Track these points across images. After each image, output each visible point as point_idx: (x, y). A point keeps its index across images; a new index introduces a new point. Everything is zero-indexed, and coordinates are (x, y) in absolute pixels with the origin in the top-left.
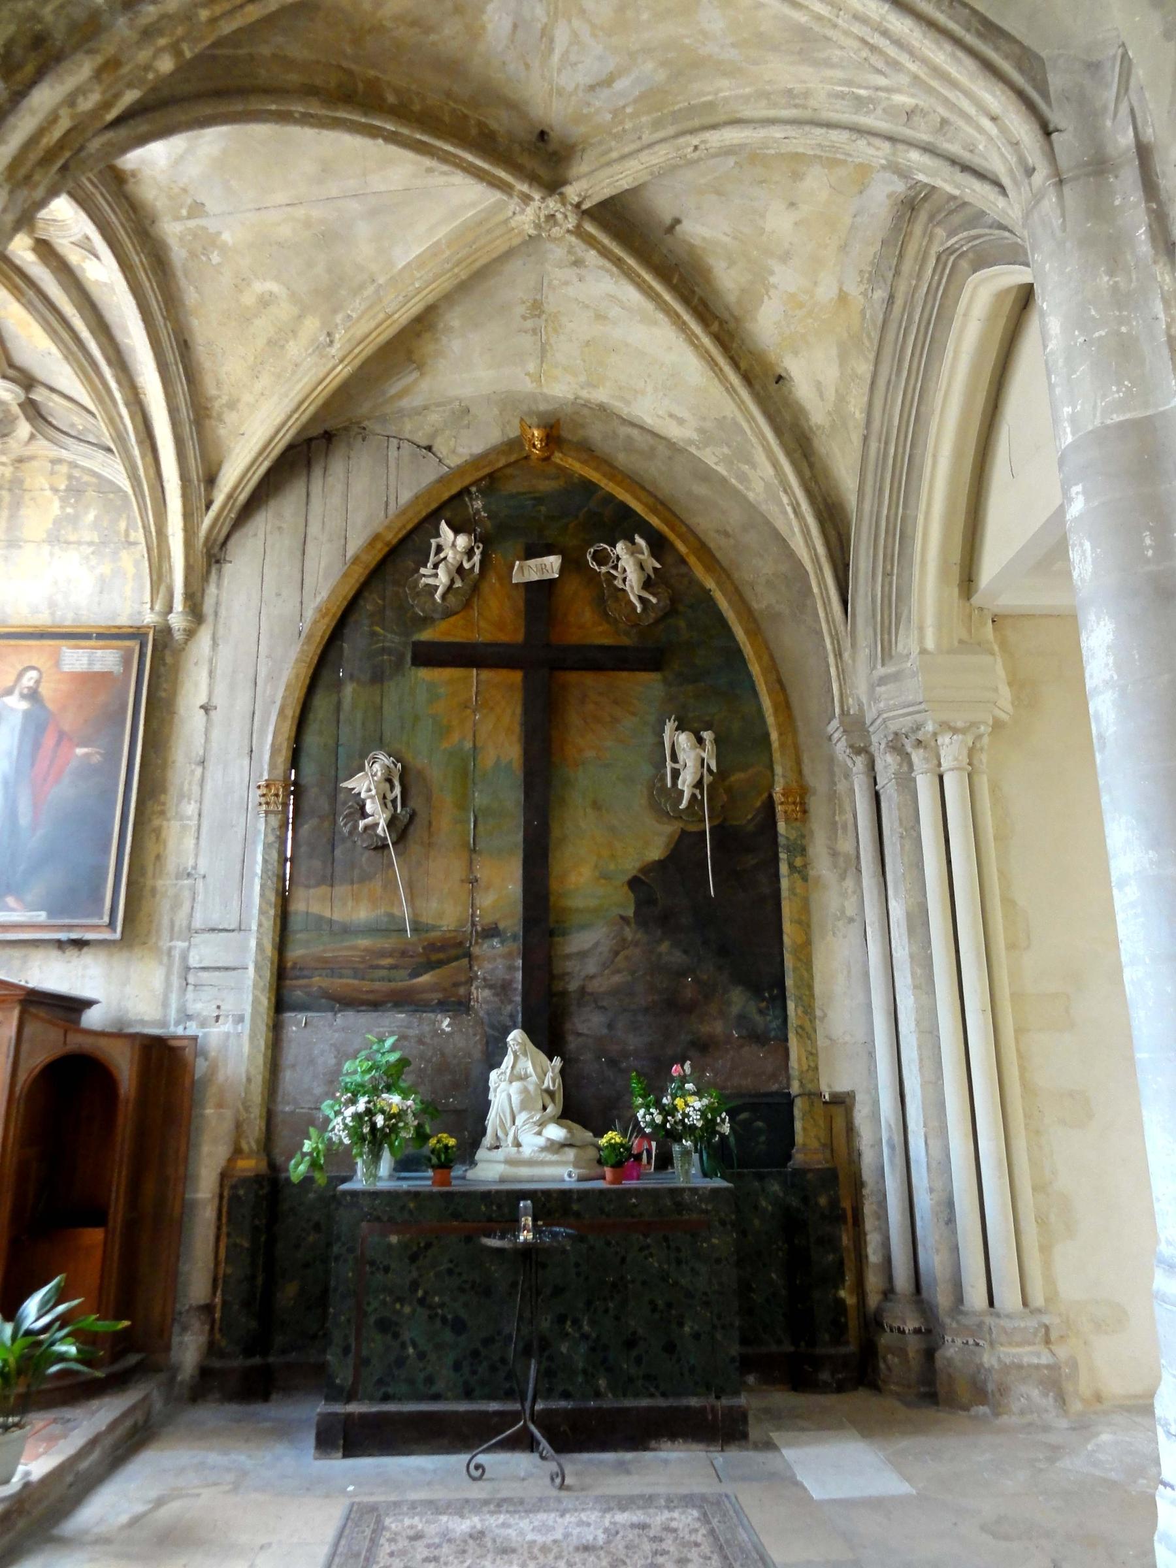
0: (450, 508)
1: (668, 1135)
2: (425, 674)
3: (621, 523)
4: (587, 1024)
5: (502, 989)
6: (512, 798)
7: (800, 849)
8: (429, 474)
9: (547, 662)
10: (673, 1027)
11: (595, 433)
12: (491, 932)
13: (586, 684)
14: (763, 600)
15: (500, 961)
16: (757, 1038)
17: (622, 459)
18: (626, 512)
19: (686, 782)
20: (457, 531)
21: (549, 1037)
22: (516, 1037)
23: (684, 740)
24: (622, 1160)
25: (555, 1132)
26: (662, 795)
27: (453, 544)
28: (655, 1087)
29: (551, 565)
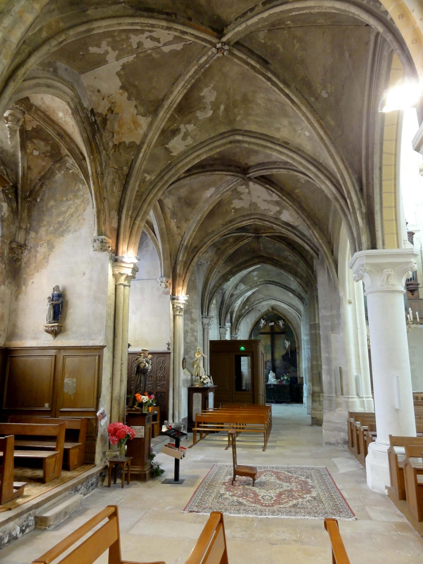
0: (262, 317)
1: (284, 380)
2: (261, 335)
3: (280, 318)
4: (277, 370)
5: (270, 367)
6: (270, 348)
7: (299, 353)
8: (260, 313)
9: (273, 334)
10: (286, 370)
11: (277, 308)
12: (268, 361)
13: (277, 336)
14: (295, 326)
15: (269, 364)
16: (294, 371)
17: (280, 311)
18: (280, 317)
19: (287, 346)
20: (263, 320)
21: (274, 371)
22: (271, 371)
23: (287, 342)
24: (279, 382)
25: (275, 380)
26: (285, 348)
27: (263, 322)
28: (283, 376)
29: (273, 324)
